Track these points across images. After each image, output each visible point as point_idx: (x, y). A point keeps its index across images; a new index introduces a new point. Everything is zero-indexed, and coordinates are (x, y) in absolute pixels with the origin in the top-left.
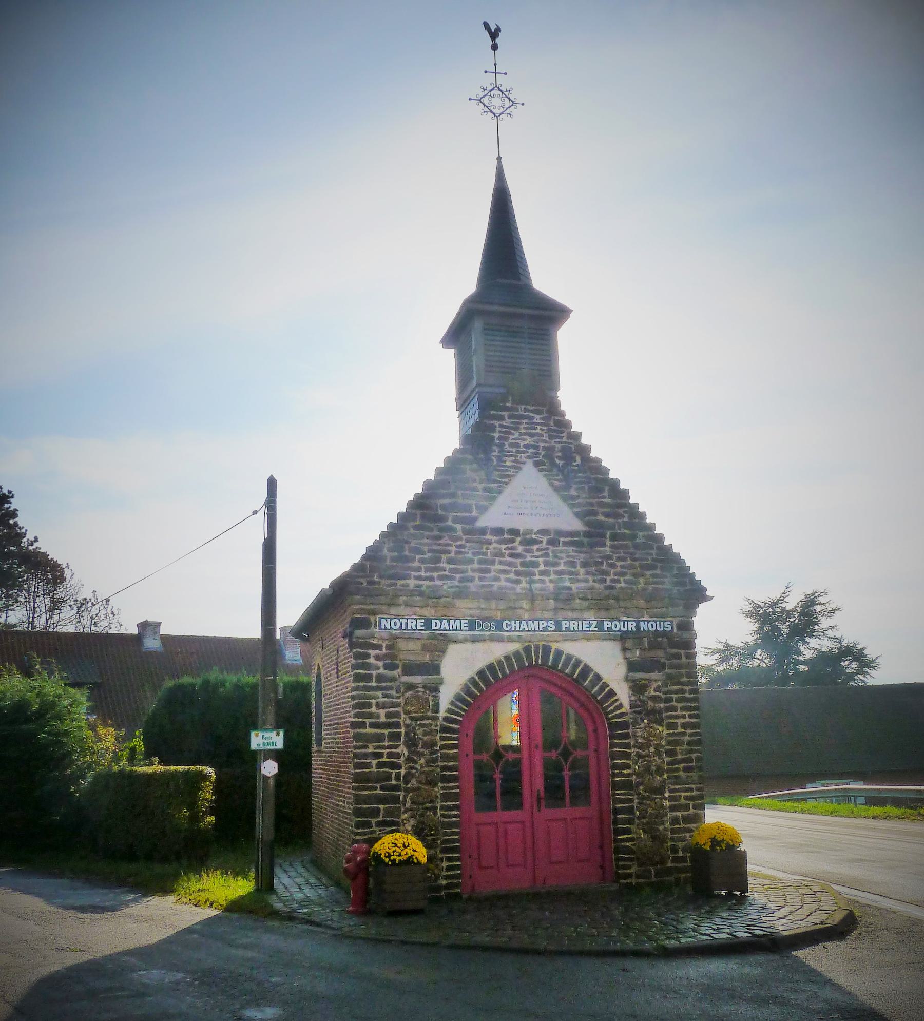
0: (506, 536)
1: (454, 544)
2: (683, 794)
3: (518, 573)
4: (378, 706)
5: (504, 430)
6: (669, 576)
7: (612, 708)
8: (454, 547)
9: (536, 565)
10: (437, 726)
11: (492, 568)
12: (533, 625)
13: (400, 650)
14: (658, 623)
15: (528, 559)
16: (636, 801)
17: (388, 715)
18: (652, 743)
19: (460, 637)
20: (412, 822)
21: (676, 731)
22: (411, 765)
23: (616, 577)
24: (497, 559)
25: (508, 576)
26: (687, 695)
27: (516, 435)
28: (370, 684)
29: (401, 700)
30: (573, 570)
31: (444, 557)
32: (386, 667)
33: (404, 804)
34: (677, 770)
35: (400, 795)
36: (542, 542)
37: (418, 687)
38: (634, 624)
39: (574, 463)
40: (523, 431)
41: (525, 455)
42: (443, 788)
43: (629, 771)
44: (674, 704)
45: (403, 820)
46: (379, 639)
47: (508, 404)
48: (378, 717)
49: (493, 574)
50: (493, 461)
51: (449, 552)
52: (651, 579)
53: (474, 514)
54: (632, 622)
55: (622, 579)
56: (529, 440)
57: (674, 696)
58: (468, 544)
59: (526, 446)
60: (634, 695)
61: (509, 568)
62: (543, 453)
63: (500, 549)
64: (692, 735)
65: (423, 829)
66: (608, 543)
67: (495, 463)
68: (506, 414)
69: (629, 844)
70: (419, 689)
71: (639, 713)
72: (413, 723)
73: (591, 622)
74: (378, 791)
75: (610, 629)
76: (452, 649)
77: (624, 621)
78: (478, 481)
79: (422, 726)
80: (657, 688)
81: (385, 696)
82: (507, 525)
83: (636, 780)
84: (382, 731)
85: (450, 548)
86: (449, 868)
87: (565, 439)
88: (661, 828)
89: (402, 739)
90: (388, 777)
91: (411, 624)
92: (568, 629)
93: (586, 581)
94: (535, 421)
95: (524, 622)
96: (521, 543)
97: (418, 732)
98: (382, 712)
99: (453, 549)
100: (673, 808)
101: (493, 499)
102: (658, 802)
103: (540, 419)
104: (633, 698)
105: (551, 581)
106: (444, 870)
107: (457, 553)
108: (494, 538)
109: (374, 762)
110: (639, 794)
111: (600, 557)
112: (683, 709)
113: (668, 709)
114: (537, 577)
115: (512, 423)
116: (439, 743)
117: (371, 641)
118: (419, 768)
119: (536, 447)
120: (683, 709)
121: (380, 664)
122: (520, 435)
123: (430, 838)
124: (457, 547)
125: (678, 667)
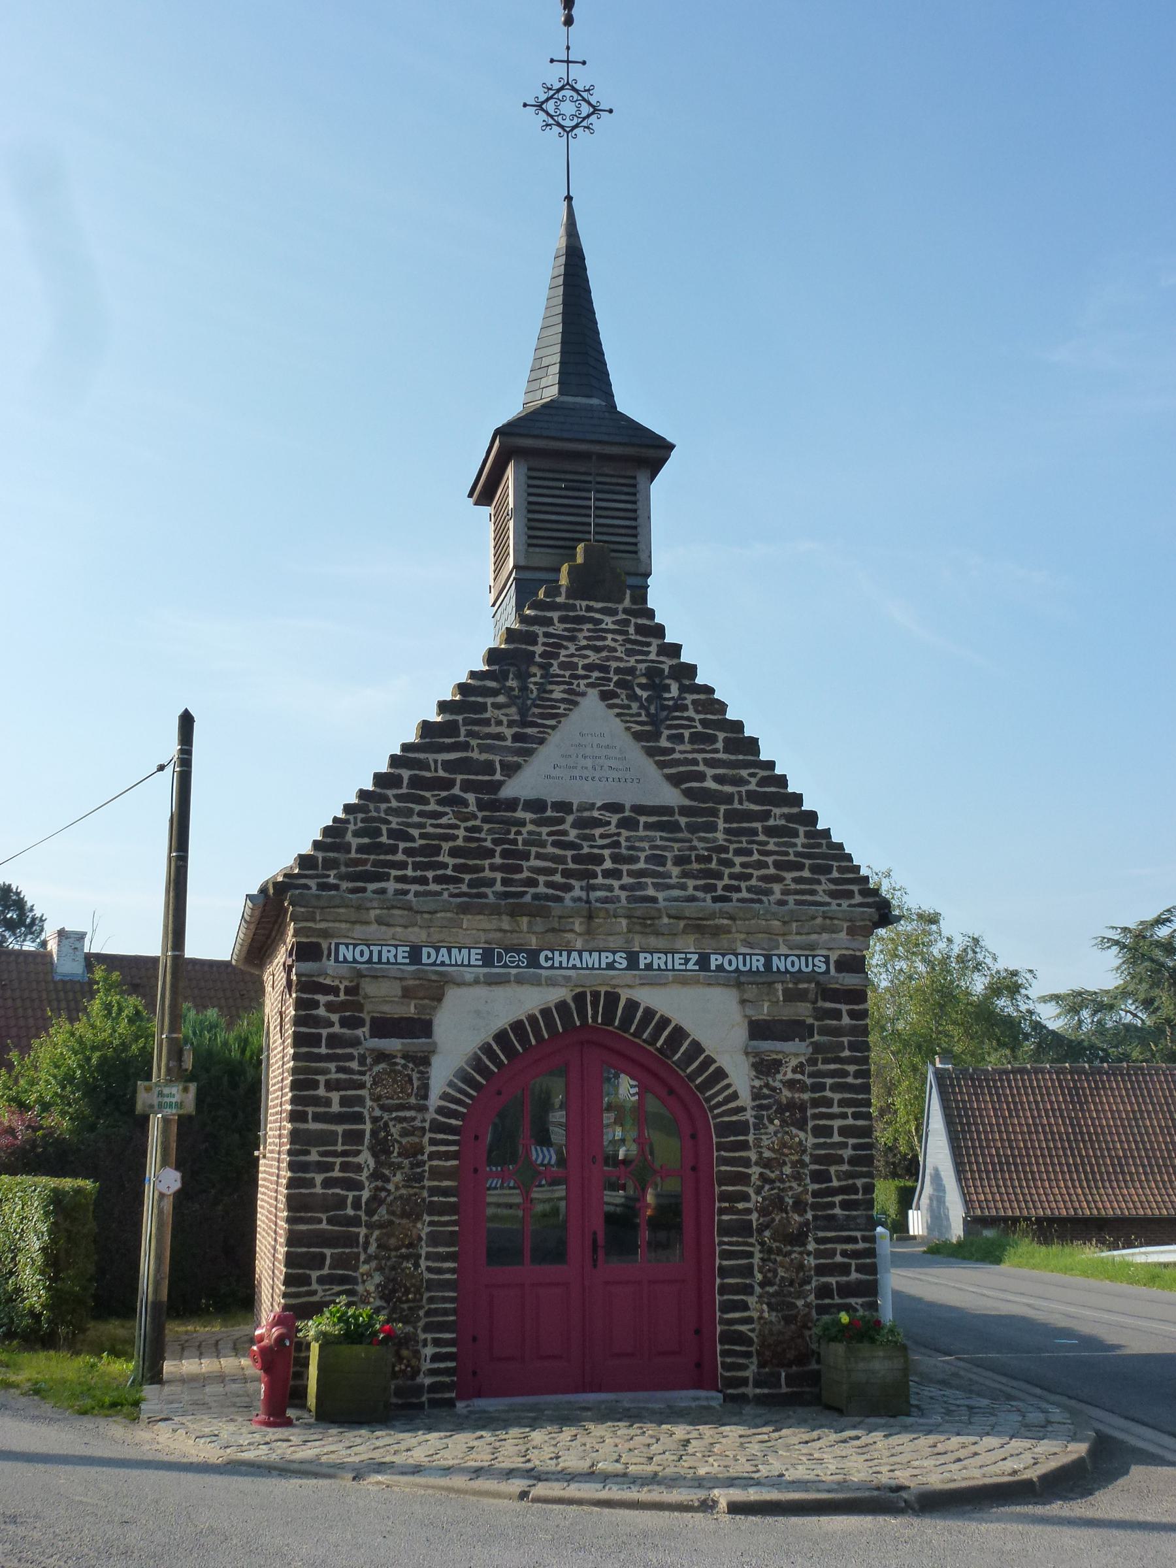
0: (549, 813)
1: (463, 825)
2: (839, 1247)
3: (566, 874)
4: (330, 1086)
5: (552, 641)
6: (823, 881)
7: (720, 1098)
8: (462, 830)
9: (600, 860)
10: (424, 1121)
11: (525, 864)
12: (591, 959)
13: (366, 997)
14: (803, 959)
15: (586, 850)
16: (758, 1255)
17: (344, 1101)
18: (787, 1159)
19: (469, 977)
20: (378, 1278)
21: (828, 1141)
22: (379, 1183)
23: (734, 882)
24: (534, 850)
25: (550, 878)
26: (850, 1080)
27: (572, 650)
28: (316, 1050)
29: (367, 1079)
30: (661, 869)
31: (446, 846)
32: (344, 1023)
33: (365, 1249)
34: (832, 1205)
35: (359, 1233)
36: (609, 823)
37: (395, 1057)
38: (762, 959)
39: (667, 695)
40: (584, 643)
41: (586, 681)
42: (431, 1223)
43: (747, 1205)
44: (828, 1094)
45: (363, 1275)
46: (333, 977)
47: (558, 600)
48: (328, 1102)
49: (525, 874)
50: (532, 692)
51: (454, 838)
52: (793, 886)
53: (498, 776)
54: (758, 957)
55: (743, 885)
56: (593, 657)
57: (829, 1081)
58: (486, 827)
59: (589, 667)
60: (758, 1078)
61: (554, 866)
62: (615, 678)
63: (540, 834)
64: (855, 1147)
65: (394, 1291)
66: (721, 825)
67: (535, 693)
68: (555, 615)
69: (743, 1328)
70: (398, 1060)
71: (767, 1107)
72: (386, 1116)
73: (689, 956)
74: (324, 1226)
75: (720, 968)
76: (453, 996)
77: (744, 955)
78: (505, 723)
79: (400, 1120)
80: (797, 1067)
81: (340, 1070)
82: (553, 795)
83: (758, 1220)
84: (333, 1127)
85: (456, 832)
86: (436, 1358)
87: (653, 657)
88: (800, 1303)
89: (366, 1142)
90: (341, 1203)
91: (388, 954)
92: (649, 967)
93: (683, 887)
94: (603, 626)
95: (575, 954)
96: (574, 826)
97: (393, 1130)
98: (335, 1097)
99: (461, 833)
100: (821, 1270)
101: (529, 753)
102: (796, 1258)
103: (614, 623)
104: (757, 1083)
105: (622, 888)
106: (428, 1360)
107: (467, 839)
108: (528, 816)
109: (319, 1178)
110: (762, 1244)
111: (707, 849)
112: (842, 1103)
113: (816, 1103)
114: (600, 880)
115: (565, 630)
116: (429, 1149)
117: (321, 980)
118: (393, 1190)
119: (604, 669)
120: (843, 1103)
121: (335, 1017)
122: (579, 649)
123: (405, 1306)
124: (467, 829)
125: (837, 1032)
